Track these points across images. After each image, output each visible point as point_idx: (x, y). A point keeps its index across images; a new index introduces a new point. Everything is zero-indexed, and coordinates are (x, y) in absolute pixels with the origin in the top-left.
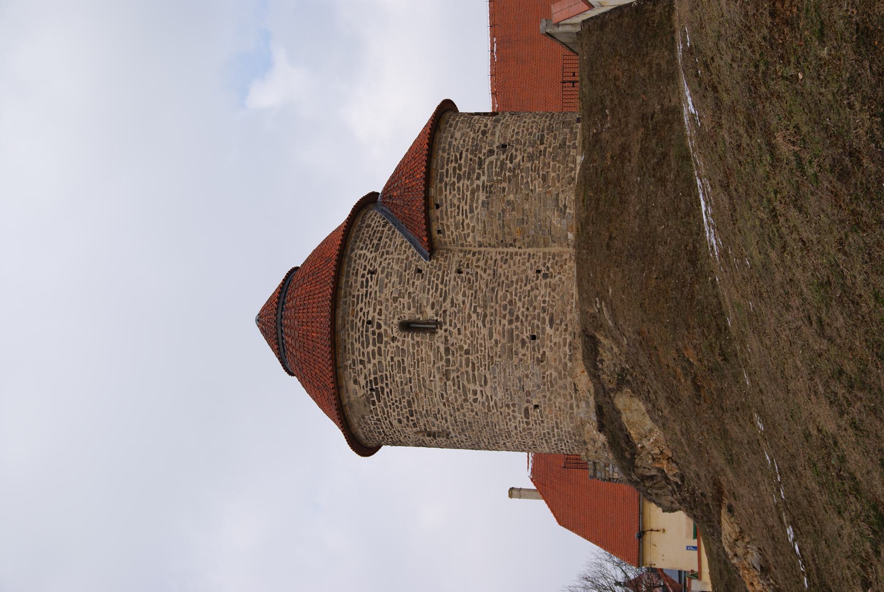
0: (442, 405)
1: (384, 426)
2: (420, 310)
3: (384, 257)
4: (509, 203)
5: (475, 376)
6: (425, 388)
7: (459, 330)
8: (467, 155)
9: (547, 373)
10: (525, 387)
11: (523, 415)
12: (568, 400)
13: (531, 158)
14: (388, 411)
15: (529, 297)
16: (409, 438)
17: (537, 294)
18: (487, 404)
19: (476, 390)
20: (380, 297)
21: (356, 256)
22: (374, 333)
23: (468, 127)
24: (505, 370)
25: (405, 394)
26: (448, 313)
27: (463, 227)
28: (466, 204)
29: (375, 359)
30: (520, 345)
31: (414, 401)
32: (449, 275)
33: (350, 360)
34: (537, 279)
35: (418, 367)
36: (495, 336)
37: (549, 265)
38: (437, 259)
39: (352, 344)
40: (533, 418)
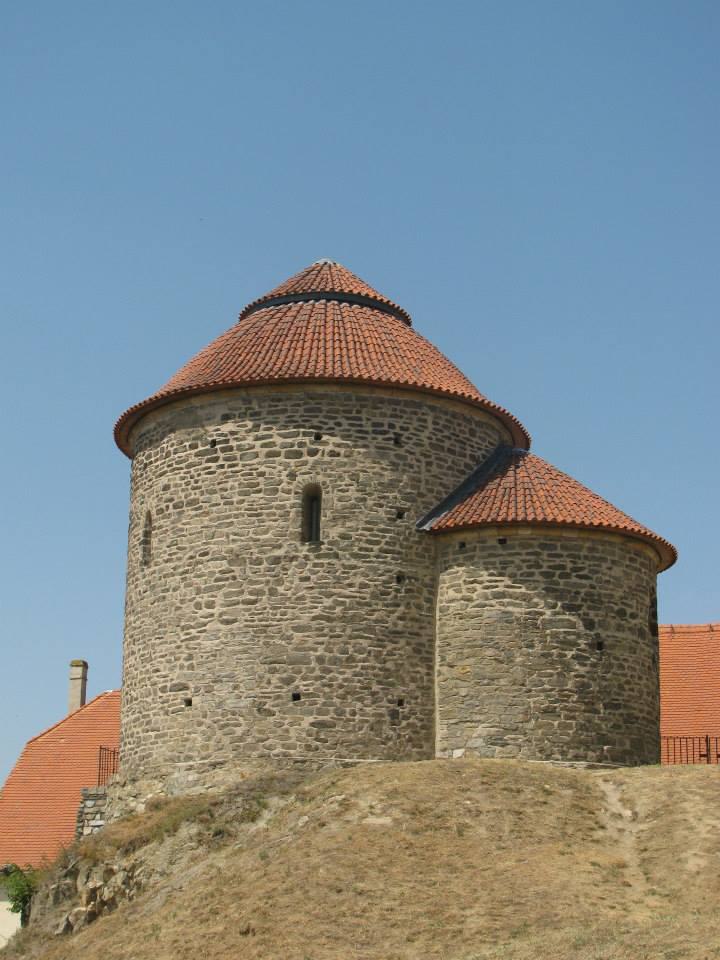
0: (191, 553)
1: (159, 463)
2: (340, 517)
3: (422, 459)
5: (235, 604)
7: (307, 579)
8: (584, 586)
9: (241, 718)
12: (199, 752)
13: (582, 689)
14: (182, 469)
15: (361, 688)
16: (142, 503)
17: (365, 702)
18: (192, 624)
19: (213, 608)
20: (359, 453)
21: (423, 414)
22: (301, 445)
23: (630, 588)
24: (245, 652)
26: (334, 561)
27: (472, 582)
28: (508, 587)
29: (263, 446)
30: (285, 675)
31: (196, 509)
32: (393, 562)
33: (260, 407)
34: (390, 701)
36: (298, 636)
37: (411, 720)
38: (419, 543)
39: (284, 411)
40: (171, 698)
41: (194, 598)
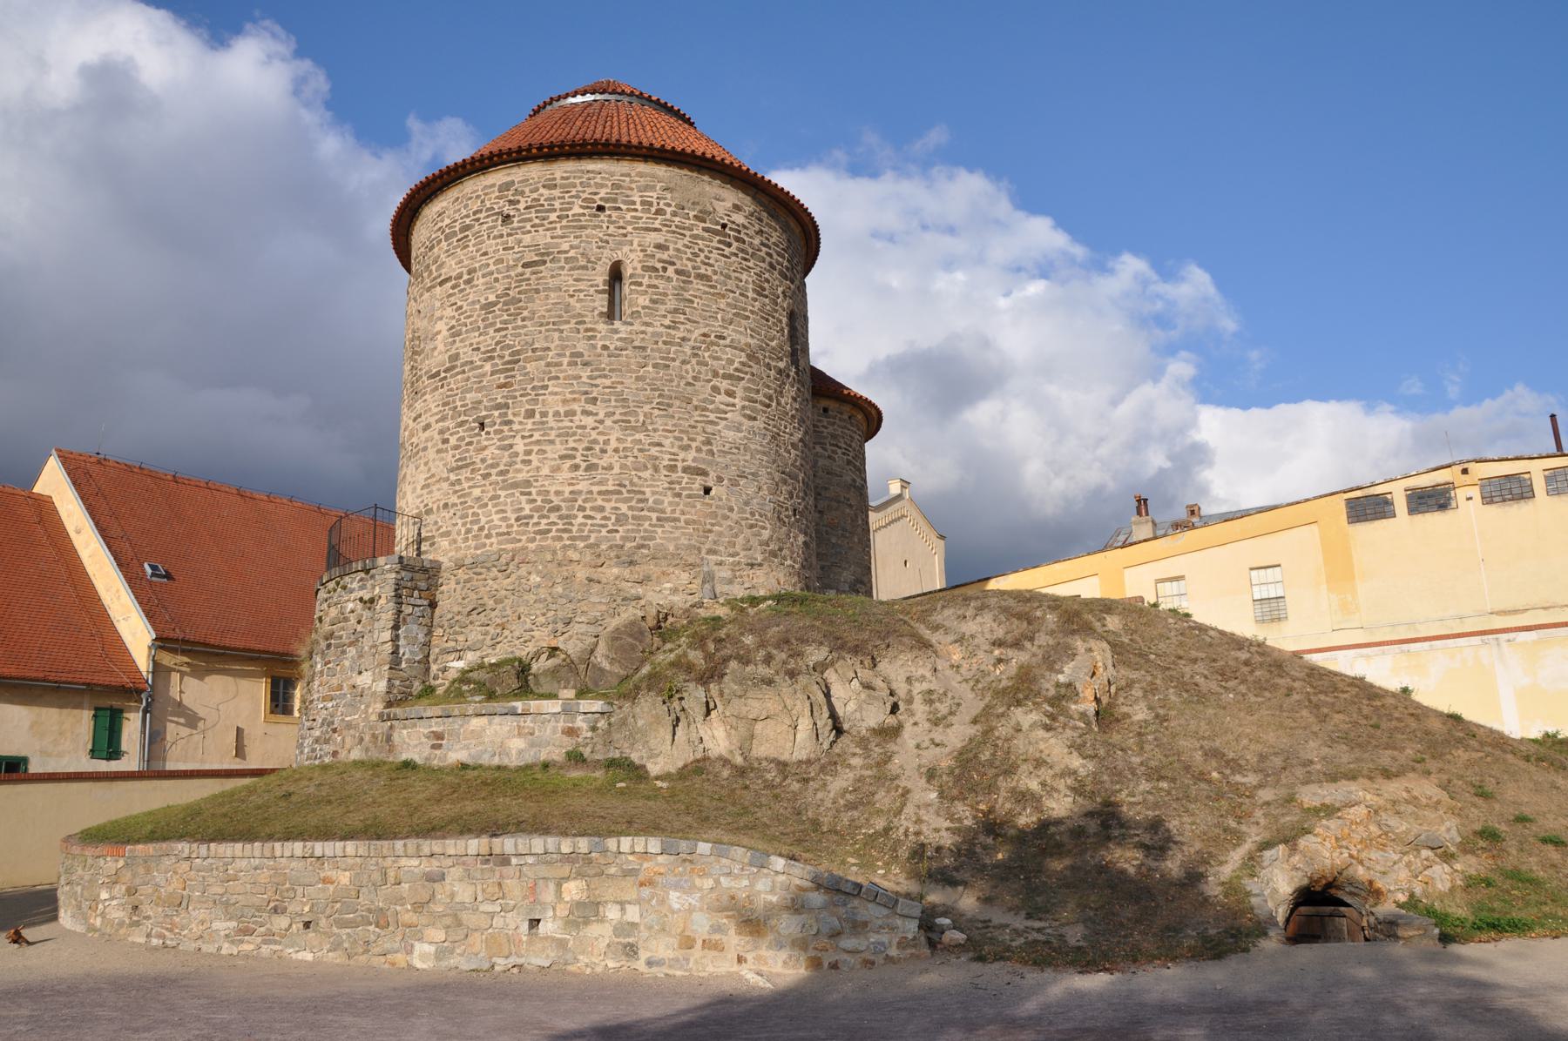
0: (706, 330)
4: (856, 515)
6: (734, 314)
10: (745, 480)
11: (689, 463)
18: (711, 407)
19: (735, 398)
25: (722, 278)
27: (833, 445)
31: (711, 287)
35: (762, 317)
39: (776, 231)
41: (711, 380)
